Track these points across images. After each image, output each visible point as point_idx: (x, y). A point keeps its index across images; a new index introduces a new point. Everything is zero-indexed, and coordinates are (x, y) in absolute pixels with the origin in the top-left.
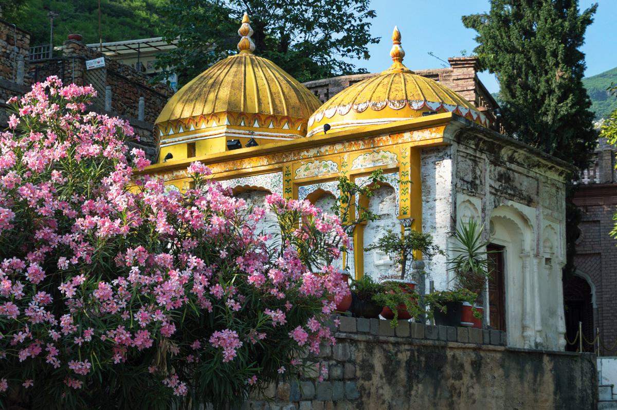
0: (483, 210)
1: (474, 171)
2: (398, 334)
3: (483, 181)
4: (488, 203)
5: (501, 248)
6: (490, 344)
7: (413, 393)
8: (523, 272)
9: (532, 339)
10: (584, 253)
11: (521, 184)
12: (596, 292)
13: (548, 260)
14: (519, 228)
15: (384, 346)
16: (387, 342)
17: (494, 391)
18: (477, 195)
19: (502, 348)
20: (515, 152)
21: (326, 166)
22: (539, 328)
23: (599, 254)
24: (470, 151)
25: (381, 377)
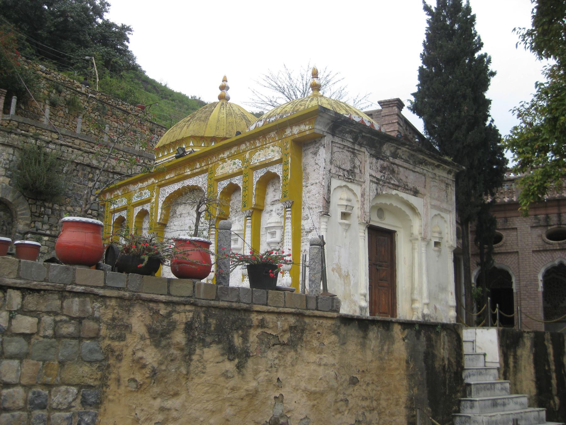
0: (363, 195)
1: (352, 161)
2: (173, 292)
3: (363, 171)
4: (367, 189)
5: (390, 234)
6: (317, 309)
7: (195, 357)
8: (413, 253)
9: (420, 310)
10: (505, 251)
11: (407, 177)
12: (516, 280)
13: (437, 244)
14: (407, 215)
15: (151, 305)
16: (156, 302)
17: (321, 359)
18: (355, 182)
19: (335, 315)
20: (397, 148)
21: (234, 164)
22: (426, 301)
23: (517, 252)
24: (349, 145)
25: (142, 338)
